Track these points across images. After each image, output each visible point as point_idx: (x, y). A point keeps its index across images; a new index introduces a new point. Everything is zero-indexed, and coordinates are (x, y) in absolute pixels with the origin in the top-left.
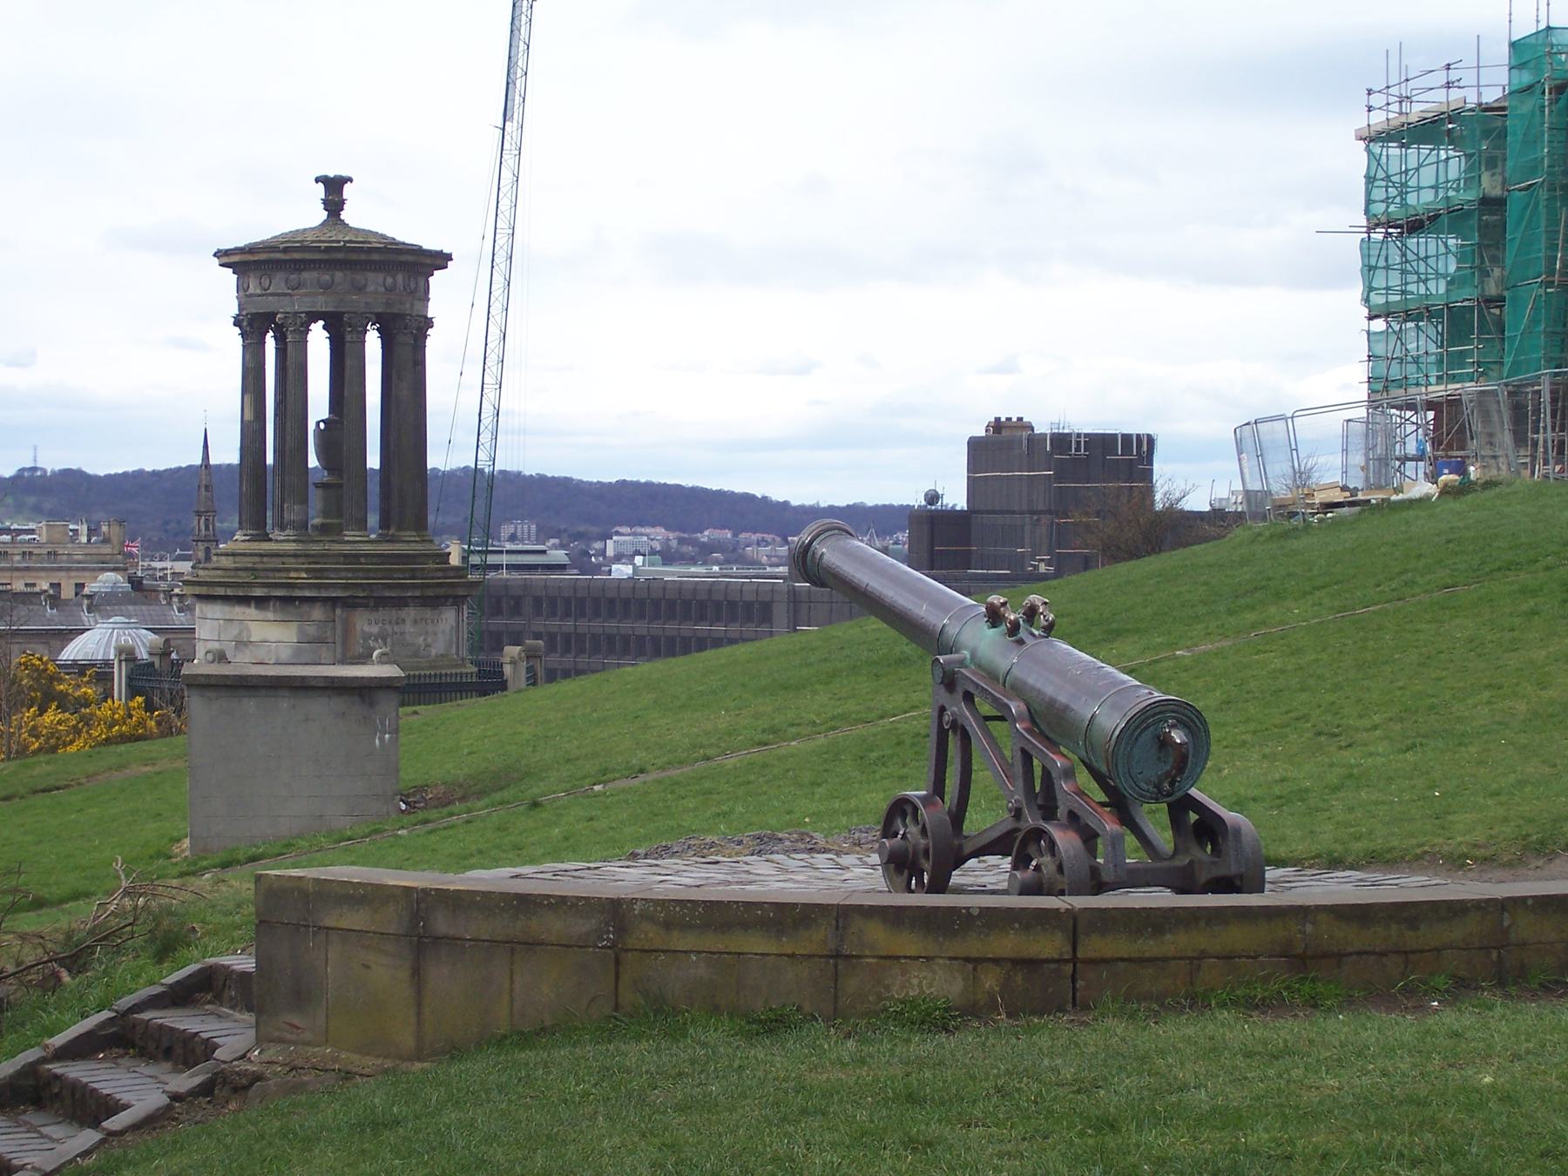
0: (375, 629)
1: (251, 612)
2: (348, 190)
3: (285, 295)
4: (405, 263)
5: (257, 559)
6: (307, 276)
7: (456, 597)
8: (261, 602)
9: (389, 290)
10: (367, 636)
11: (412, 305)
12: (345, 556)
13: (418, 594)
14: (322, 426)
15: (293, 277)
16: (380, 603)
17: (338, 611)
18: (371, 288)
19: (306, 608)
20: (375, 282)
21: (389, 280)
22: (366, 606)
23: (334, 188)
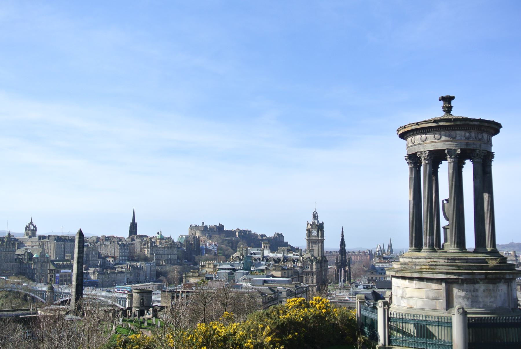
1: (406, 282)
2: (453, 103)
3: (420, 144)
4: (474, 125)
5: (410, 260)
7: (506, 279)
8: (411, 279)
9: (468, 138)
11: (480, 146)
12: (448, 259)
13: (483, 277)
16: (463, 281)
20: (460, 134)
21: (467, 134)
23: (447, 100)
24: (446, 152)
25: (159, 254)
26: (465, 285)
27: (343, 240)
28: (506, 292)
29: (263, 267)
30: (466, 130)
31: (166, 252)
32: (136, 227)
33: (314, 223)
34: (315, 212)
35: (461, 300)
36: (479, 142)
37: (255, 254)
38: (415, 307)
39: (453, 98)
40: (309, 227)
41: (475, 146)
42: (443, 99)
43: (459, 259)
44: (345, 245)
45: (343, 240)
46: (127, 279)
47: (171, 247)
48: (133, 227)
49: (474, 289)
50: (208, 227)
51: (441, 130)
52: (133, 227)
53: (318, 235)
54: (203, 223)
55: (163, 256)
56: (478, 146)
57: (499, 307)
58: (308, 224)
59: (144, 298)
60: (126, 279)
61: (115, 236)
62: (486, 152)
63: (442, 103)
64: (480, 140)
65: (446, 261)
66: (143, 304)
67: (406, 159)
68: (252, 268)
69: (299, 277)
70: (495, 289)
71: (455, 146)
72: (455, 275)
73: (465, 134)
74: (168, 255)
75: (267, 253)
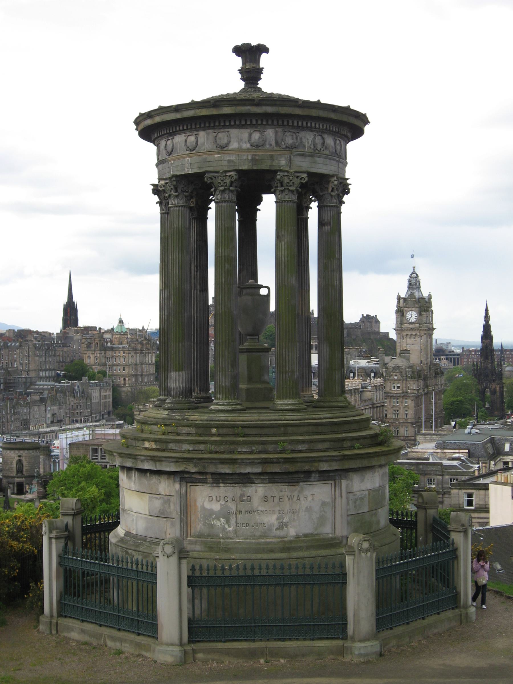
0: (216, 507)
2: (264, 60)
6: (179, 139)
9: (256, 146)
10: (209, 514)
11: (290, 160)
12: (197, 426)
15: (169, 142)
16: (219, 479)
18: (234, 145)
19: (154, 479)
21: (256, 136)
22: (204, 482)
23: (250, 55)
24: (205, 179)
25: (119, 365)
27: (487, 328)
28: (328, 500)
30: (252, 126)
31: (132, 361)
32: (76, 310)
33: (412, 295)
36: (287, 154)
38: (134, 533)
39: (262, 49)
40: (402, 304)
41: (275, 163)
42: (238, 50)
43: (217, 427)
44: (491, 338)
45: (487, 328)
46: (53, 415)
47: (141, 350)
48: (70, 311)
49: (242, 495)
51: (196, 129)
52: (70, 311)
53: (419, 322)
55: (127, 367)
56: (283, 162)
57: (306, 535)
58: (399, 298)
59: (23, 459)
60: (49, 415)
61: (34, 329)
62: (305, 175)
63: (238, 62)
64: (290, 148)
65: (193, 430)
66: (22, 472)
70: (296, 494)
71: (226, 163)
72: (195, 466)
73: (250, 135)
74: (136, 365)
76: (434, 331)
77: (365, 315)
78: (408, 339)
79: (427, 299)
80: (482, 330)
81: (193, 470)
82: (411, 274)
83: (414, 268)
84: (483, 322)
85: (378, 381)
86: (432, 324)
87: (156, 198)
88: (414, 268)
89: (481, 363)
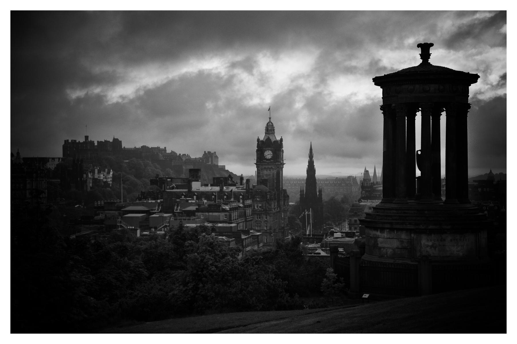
0: (430, 244)
14: (419, 153)
17: (413, 235)
26: (433, 236)
29: (193, 208)
33: (268, 139)
34: (270, 122)
35: (428, 249)
37: (178, 187)
44: (314, 171)
50: (96, 144)
54: (87, 137)
58: (258, 140)
67: (381, 109)
68: (178, 209)
69: (246, 221)
75: (196, 186)
76: (284, 166)
77: (207, 152)
78: (265, 171)
79: (279, 142)
80: (307, 164)
81: (423, 228)
82: (268, 124)
83: (270, 118)
84: (307, 159)
85: (249, 202)
86: (283, 160)
87: (382, 111)
88: (270, 118)
89: (306, 190)
